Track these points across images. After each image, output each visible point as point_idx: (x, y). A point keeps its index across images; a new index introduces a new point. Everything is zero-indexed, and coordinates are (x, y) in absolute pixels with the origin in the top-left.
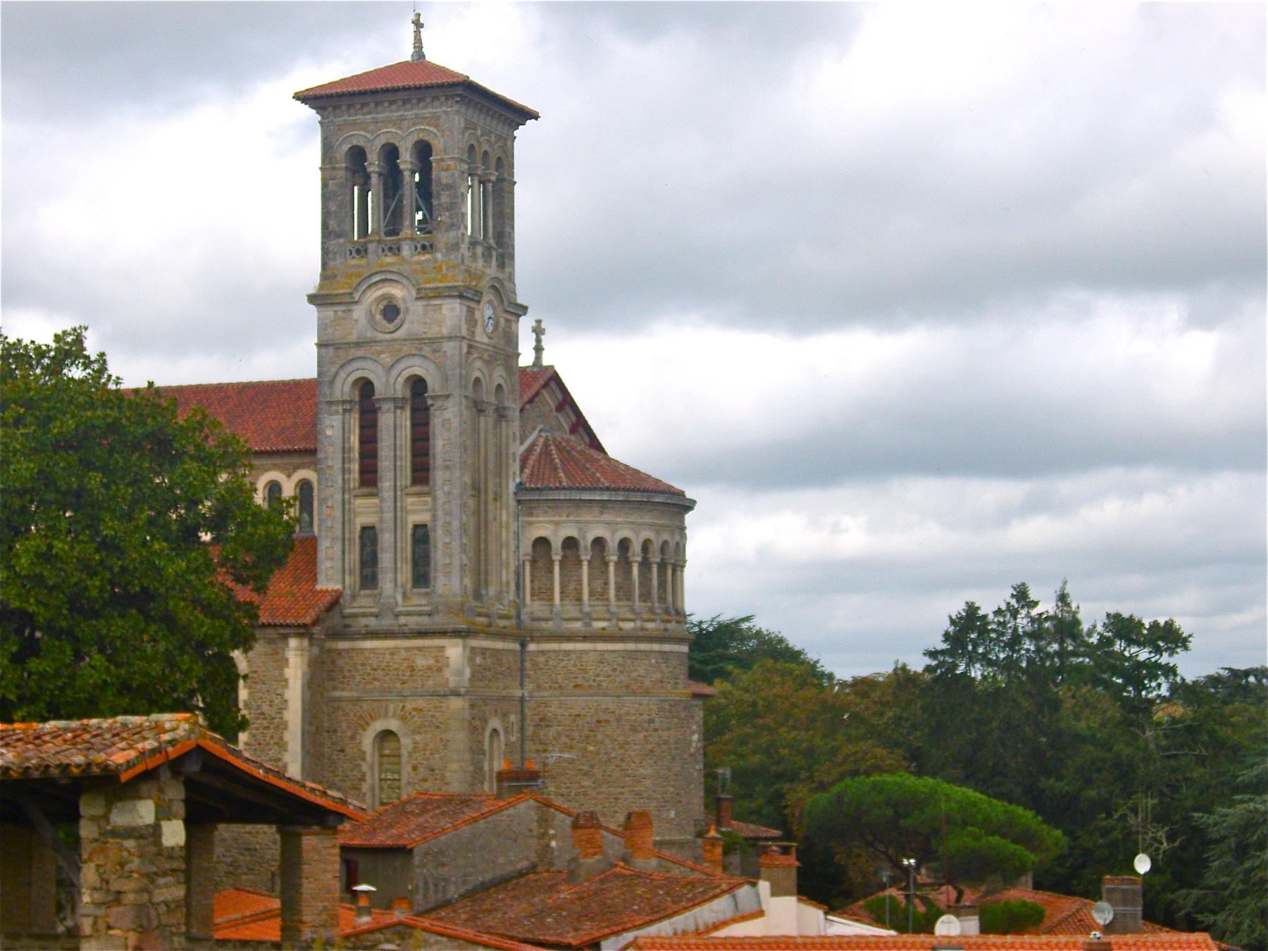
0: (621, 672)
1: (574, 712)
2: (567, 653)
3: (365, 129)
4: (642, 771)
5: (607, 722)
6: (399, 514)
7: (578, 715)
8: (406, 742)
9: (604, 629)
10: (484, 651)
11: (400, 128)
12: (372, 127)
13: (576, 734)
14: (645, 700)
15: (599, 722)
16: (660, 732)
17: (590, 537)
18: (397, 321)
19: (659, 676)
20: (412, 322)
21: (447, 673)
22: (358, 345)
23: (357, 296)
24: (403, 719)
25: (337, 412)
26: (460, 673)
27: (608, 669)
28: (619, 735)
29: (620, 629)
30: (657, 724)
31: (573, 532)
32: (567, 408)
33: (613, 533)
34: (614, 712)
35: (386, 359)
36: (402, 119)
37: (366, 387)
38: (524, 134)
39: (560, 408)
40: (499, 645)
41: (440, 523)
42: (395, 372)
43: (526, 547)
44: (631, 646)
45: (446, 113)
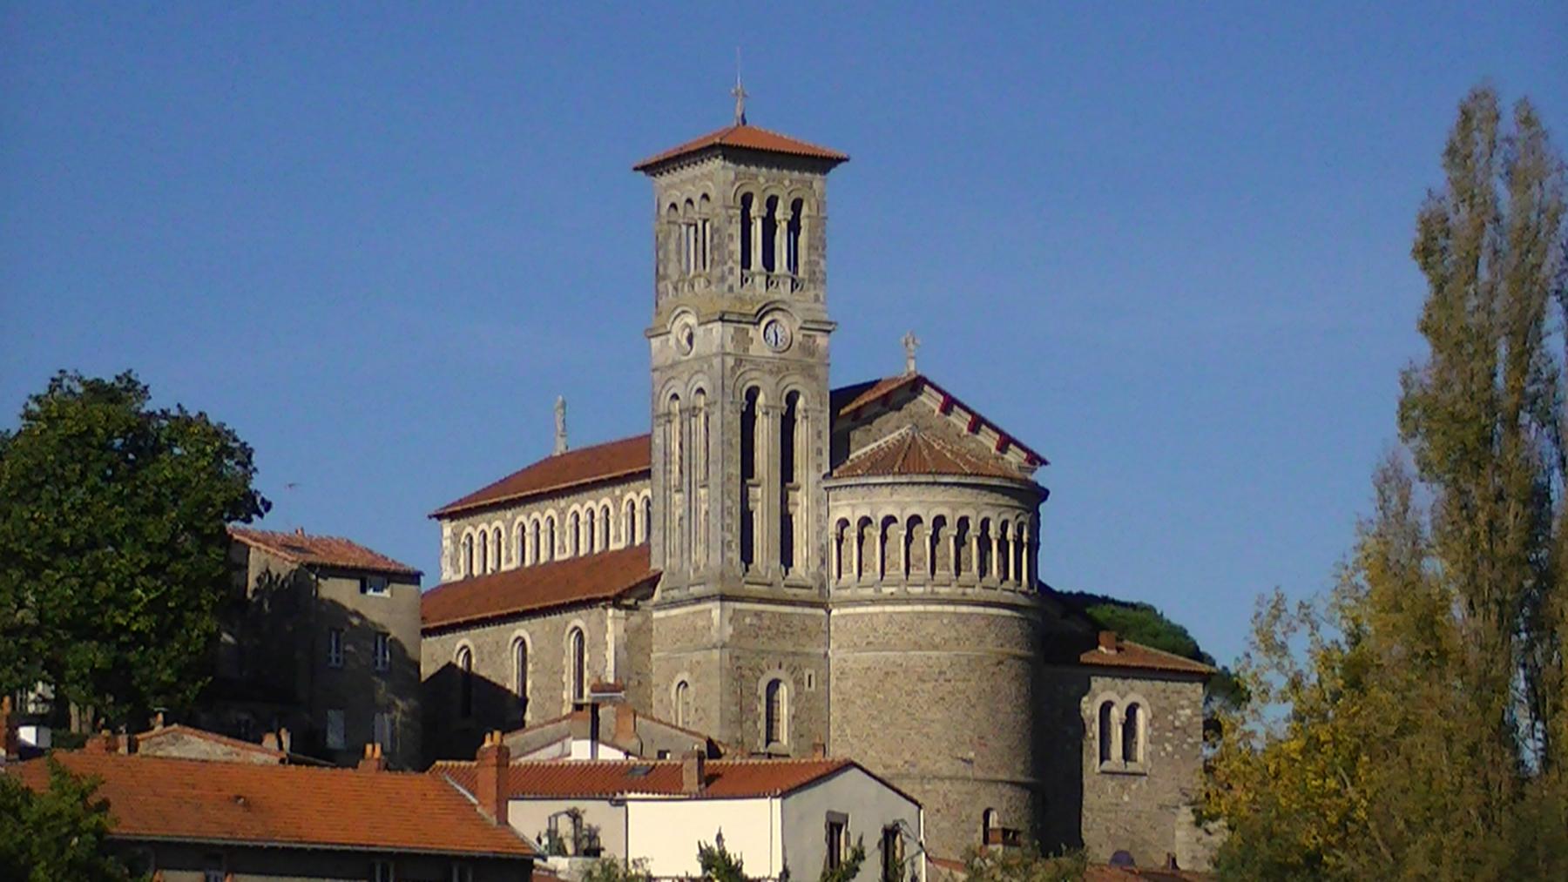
0: (909, 630)
1: (866, 666)
2: (862, 615)
4: (929, 715)
5: (895, 673)
7: (869, 668)
9: (892, 594)
13: (866, 684)
14: (934, 654)
15: (887, 673)
16: (953, 682)
19: (954, 634)
22: (672, 366)
27: (896, 629)
28: (907, 684)
29: (908, 593)
30: (948, 676)
33: (902, 510)
34: (901, 665)
43: (832, 528)
44: (920, 608)
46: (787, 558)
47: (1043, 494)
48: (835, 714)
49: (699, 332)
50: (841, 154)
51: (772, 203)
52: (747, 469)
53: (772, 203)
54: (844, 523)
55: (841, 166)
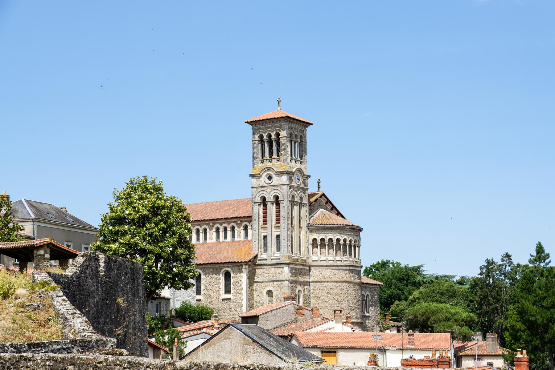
0: (337, 275)
3: (263, 130)
5: (333, 288)
6: (272, 232)
8: (274, 293)
10: (296, 269)
11: (272, 129)
12: (265, 129)
15: (331, 288)
16: (349, 291)
17: (328, 238)
18: (271, 181)
20: (275, 181)
21: (284, 274)
23: (261, 174)
24: (273, 287)
25: (256, 205)
26: (288, 274)
31: (324, 237)
32: (329, 203)
35: (269, 191)
36: (272, 127)
37: (264, 198)
38: (309, 128)
39: (326, 203)
40: (301, 267)
41: (282, 234)
42: (271, 194)
45: (283, 125)
50: (312, 123)
54: (315, 240)
55: (311, 125)
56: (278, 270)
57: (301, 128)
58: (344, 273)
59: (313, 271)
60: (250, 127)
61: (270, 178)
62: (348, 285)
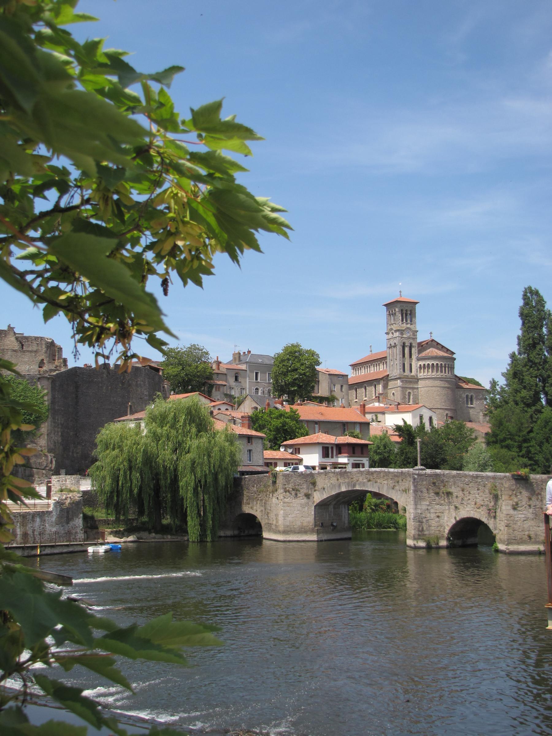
38: (417, 305)
46: (411, 371)
47: (455, 359)
48: (420, 398)
49: (394, 333)
51: (406, 311)
52: (404, 356)
53: (406, 311)
54: (420, 365)
56: (396, 382)
57: (412, 305)
58: (436, 382)
59: (420, 382)
60: (385, 307)
61: (393, 334)
62: (439, 388)
